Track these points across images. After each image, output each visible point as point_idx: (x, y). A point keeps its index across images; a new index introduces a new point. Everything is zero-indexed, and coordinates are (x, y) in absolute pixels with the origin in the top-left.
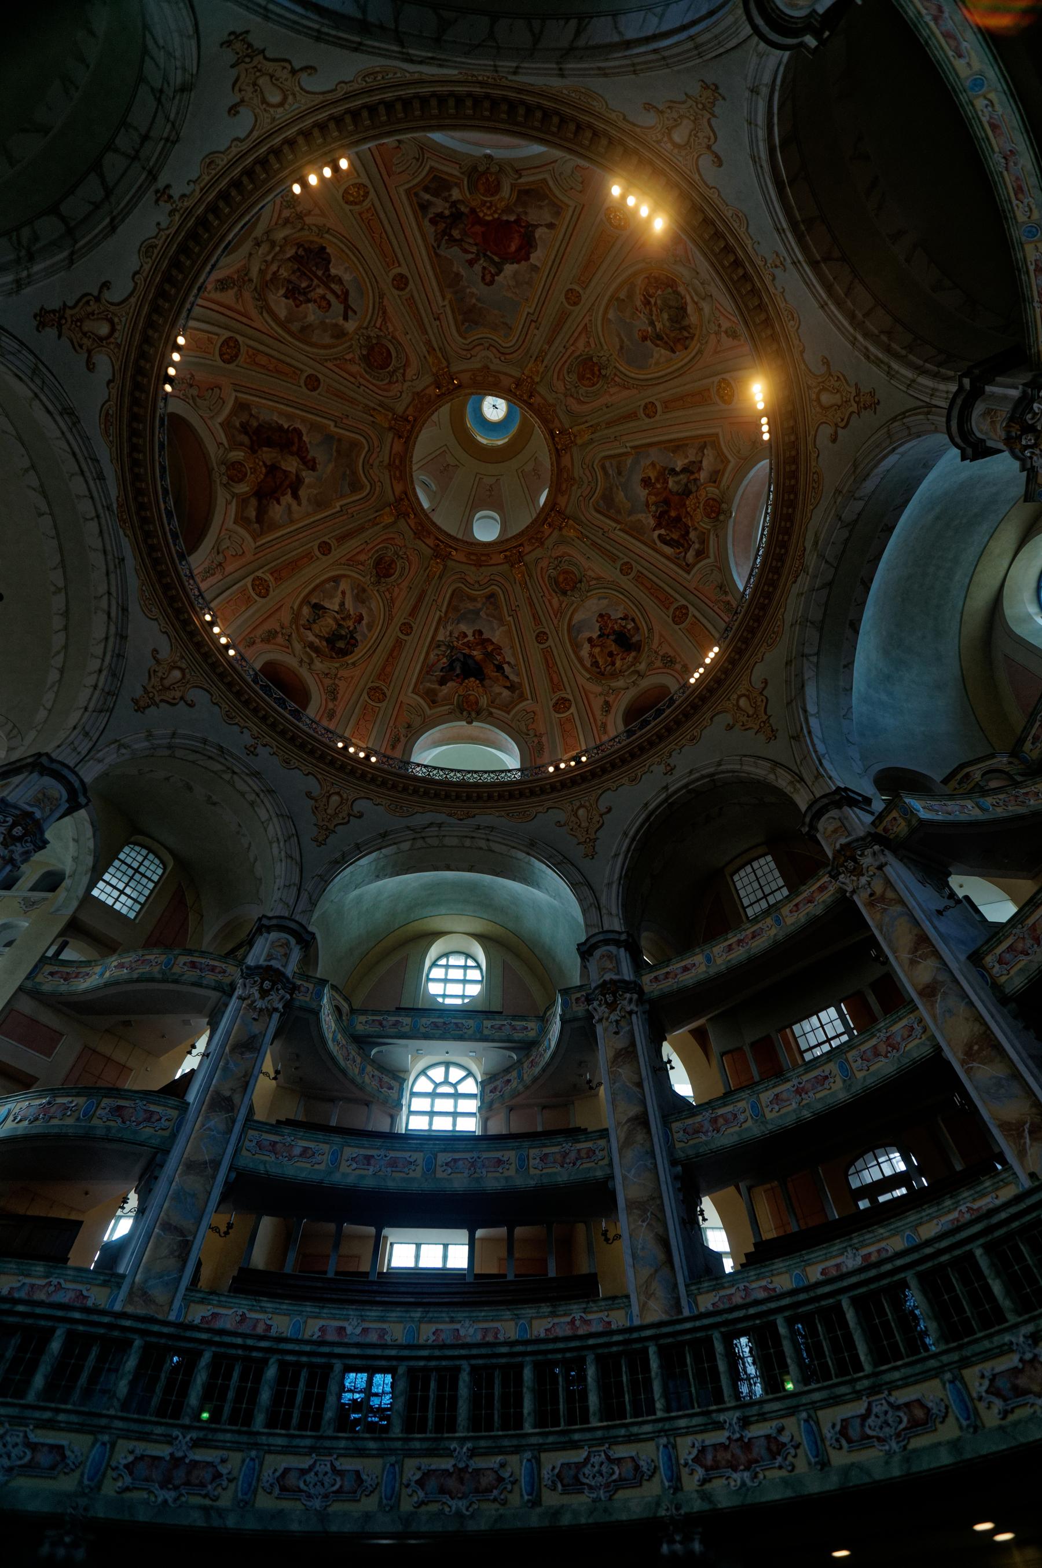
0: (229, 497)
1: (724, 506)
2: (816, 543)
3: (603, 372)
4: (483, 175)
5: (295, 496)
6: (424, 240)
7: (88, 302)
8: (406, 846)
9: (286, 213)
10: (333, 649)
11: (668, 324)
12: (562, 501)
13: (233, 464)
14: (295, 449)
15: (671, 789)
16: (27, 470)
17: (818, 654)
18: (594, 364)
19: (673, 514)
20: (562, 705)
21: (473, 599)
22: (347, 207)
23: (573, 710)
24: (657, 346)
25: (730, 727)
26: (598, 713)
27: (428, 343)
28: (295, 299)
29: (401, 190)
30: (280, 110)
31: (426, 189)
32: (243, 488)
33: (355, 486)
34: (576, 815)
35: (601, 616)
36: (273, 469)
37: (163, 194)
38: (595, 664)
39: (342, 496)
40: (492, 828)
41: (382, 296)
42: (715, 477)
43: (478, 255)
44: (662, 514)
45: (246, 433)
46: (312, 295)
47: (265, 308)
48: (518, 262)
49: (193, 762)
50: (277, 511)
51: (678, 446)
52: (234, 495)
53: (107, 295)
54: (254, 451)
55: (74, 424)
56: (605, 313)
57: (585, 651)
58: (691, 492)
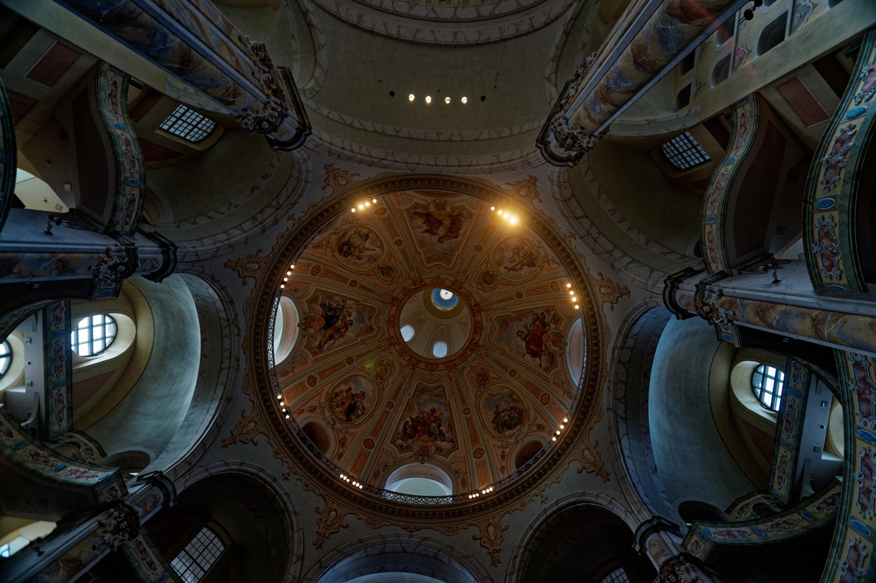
2: (425, 539)
4: (560, 339)
5: (426, 231)
8: (223, 315)
10: (344, 244)
12: (422, 365)
15: (273, 484)
16: (461, 136)
19: (419, 428)
20: (312, 381)
21: (370, 319)
25: (317, 510)
26: (309, 405)
31: (555, 314)
32: (432, 208)
33: (429, 260)
35: (364, 393)
36: (440, 223)
38: (337, 395)
39: (425, 253)
40: (238, 369)
46: (516, 256)
49: (285, 186)
50: (419, 221)
51: (451, 427)
52: (429, 204)
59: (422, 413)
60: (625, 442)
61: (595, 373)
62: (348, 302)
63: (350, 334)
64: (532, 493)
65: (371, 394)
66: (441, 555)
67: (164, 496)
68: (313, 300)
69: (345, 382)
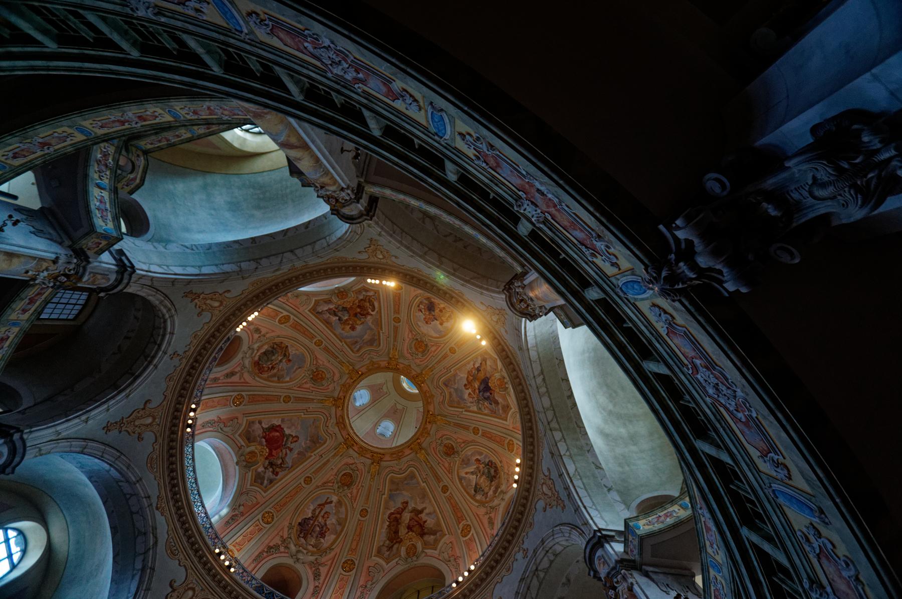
4: (246, 462)
6: (287, 475)
8: (558, 435)
9: (282, 549)
10: (495, 477)
12: (384, 364)
13: (408, 553)
14: (398, 516)
19: (359, 310)
22: (275, 519)
30: (197, 589)
31: (262, 484)
32: (419, 545)
33: (412, 476)
39: (418, 483)
41: (318, 487)
42: (328, 301)
45: (392, 547)
47: (330, 548)
50: (430, 522)
51: (327, 323)
52: (423, 552)
54: (400, 542)
59: (363, 323)
60: (107, 467)
62: (475, 409)
63: (463, 375)
64: (193, 349)
65: (419, 323)
66: (253, 265)
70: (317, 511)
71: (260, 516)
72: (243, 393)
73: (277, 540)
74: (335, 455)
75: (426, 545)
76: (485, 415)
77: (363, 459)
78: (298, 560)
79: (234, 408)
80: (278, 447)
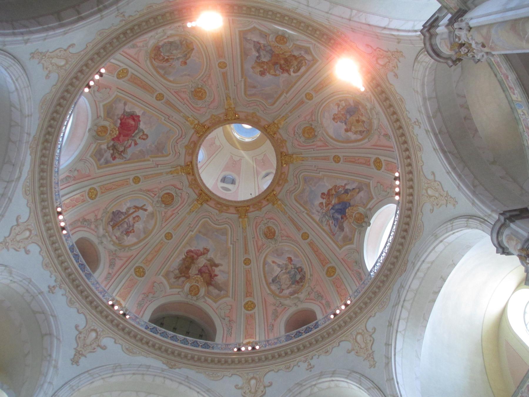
0: (203, 300)
1: (280, 33)
3: (200, 86)
5: (217, 265)
6: (121, 164)
7: (79, 338)
8: (405, 314)
9: (93, 226)
10: (298, 282)
11: (179, 51)
12: (263, 123)
13: (190, 291)
14: (195, 256)
17: (352, 9)
18: (195, 91)
19: (282, 62)
22: (97, 199)
23: (382, 158)
24: (190, 57)
25: (396, 75)
27: (167, 173)
28: (130, 232)
29: (97, 171)
30: (33, 232)
31: (99, 160)
33: (224, 233)
34: (431, 197)
35: (334, 119)
37: (51, 289)
38: (361, 132)
41: (141, 190)
43: (133, 140)
44: (281, 68)
45: (179, 277)
46: (131, 223)
48: (140, 121)
50: (220, 278)
51: (244, 53)
52: (203, 297)
53: (81, 328)
54: (188, 278)
55: (121, 368)
56: (170, 81)
57: (352, 136)
58: (271, 50)
59: (275, 75)
61: (46, 141)
62: (317, 218)
63: (327, 186)
64: (137, 16)
67: (502, 233)
68: (348, 240)
69: (348, 141)
70: (132, 211)
71: (87, 189)
72: (130, 70)
73: (91, 217)
74: (171, 173)
75: (208, 293)
76: (324, 230)
77: (190, 191)
78: (102, 242)
79: (115, 79)
80: (126, 135)
